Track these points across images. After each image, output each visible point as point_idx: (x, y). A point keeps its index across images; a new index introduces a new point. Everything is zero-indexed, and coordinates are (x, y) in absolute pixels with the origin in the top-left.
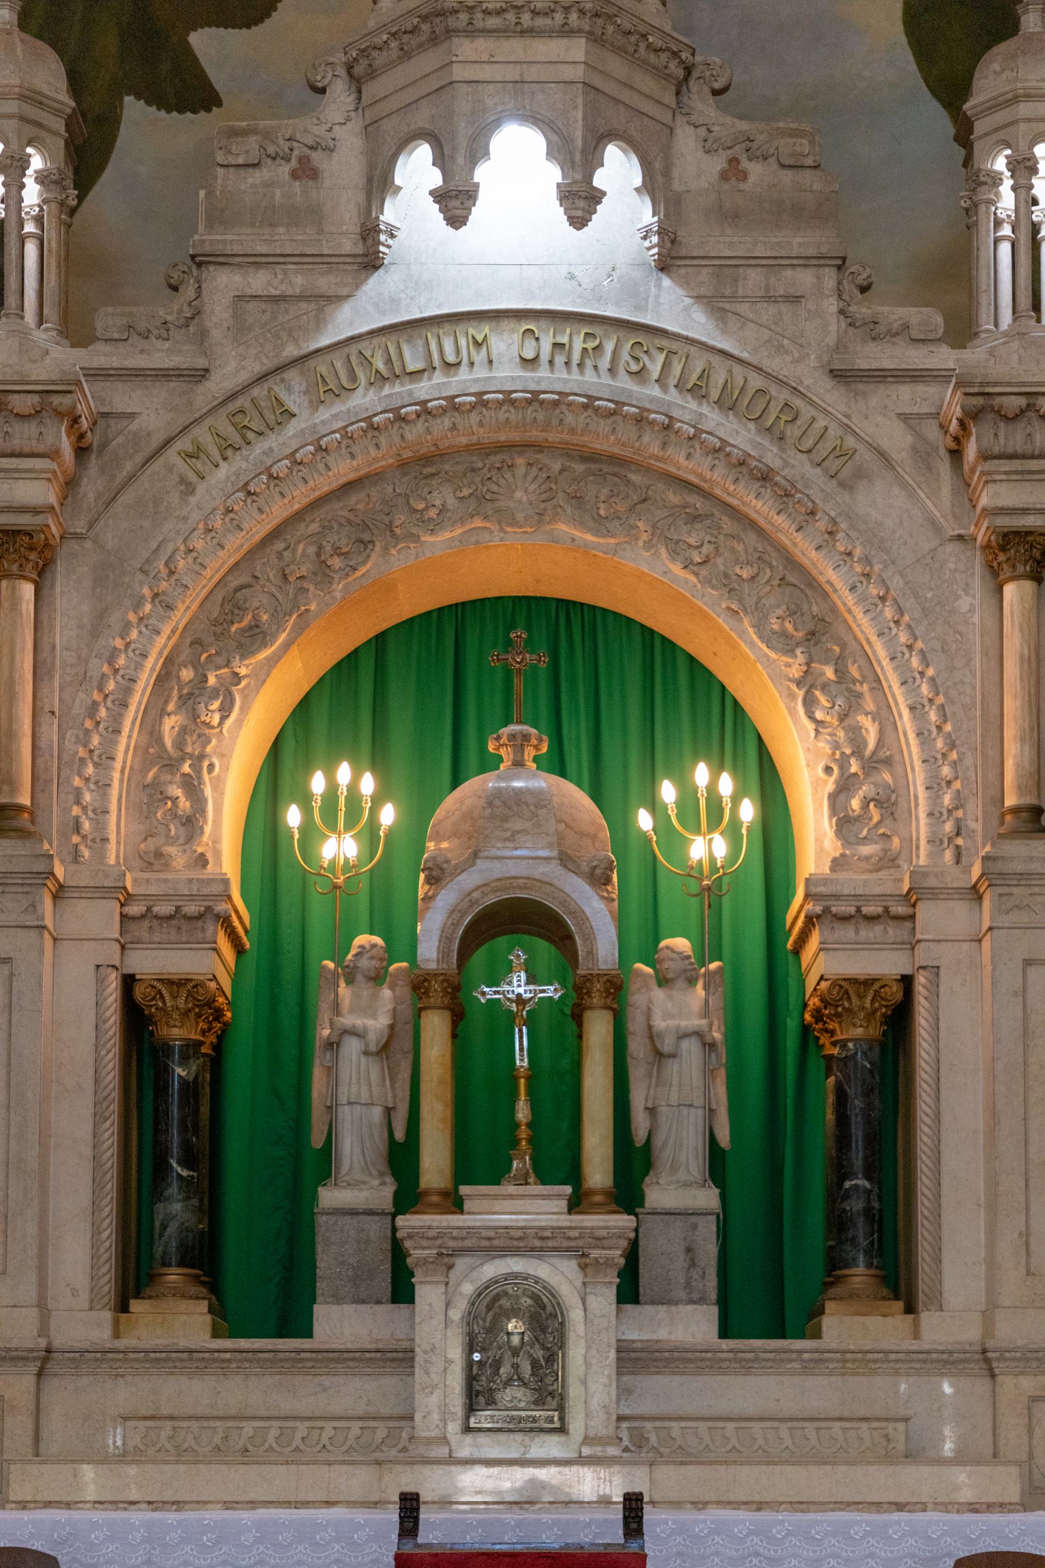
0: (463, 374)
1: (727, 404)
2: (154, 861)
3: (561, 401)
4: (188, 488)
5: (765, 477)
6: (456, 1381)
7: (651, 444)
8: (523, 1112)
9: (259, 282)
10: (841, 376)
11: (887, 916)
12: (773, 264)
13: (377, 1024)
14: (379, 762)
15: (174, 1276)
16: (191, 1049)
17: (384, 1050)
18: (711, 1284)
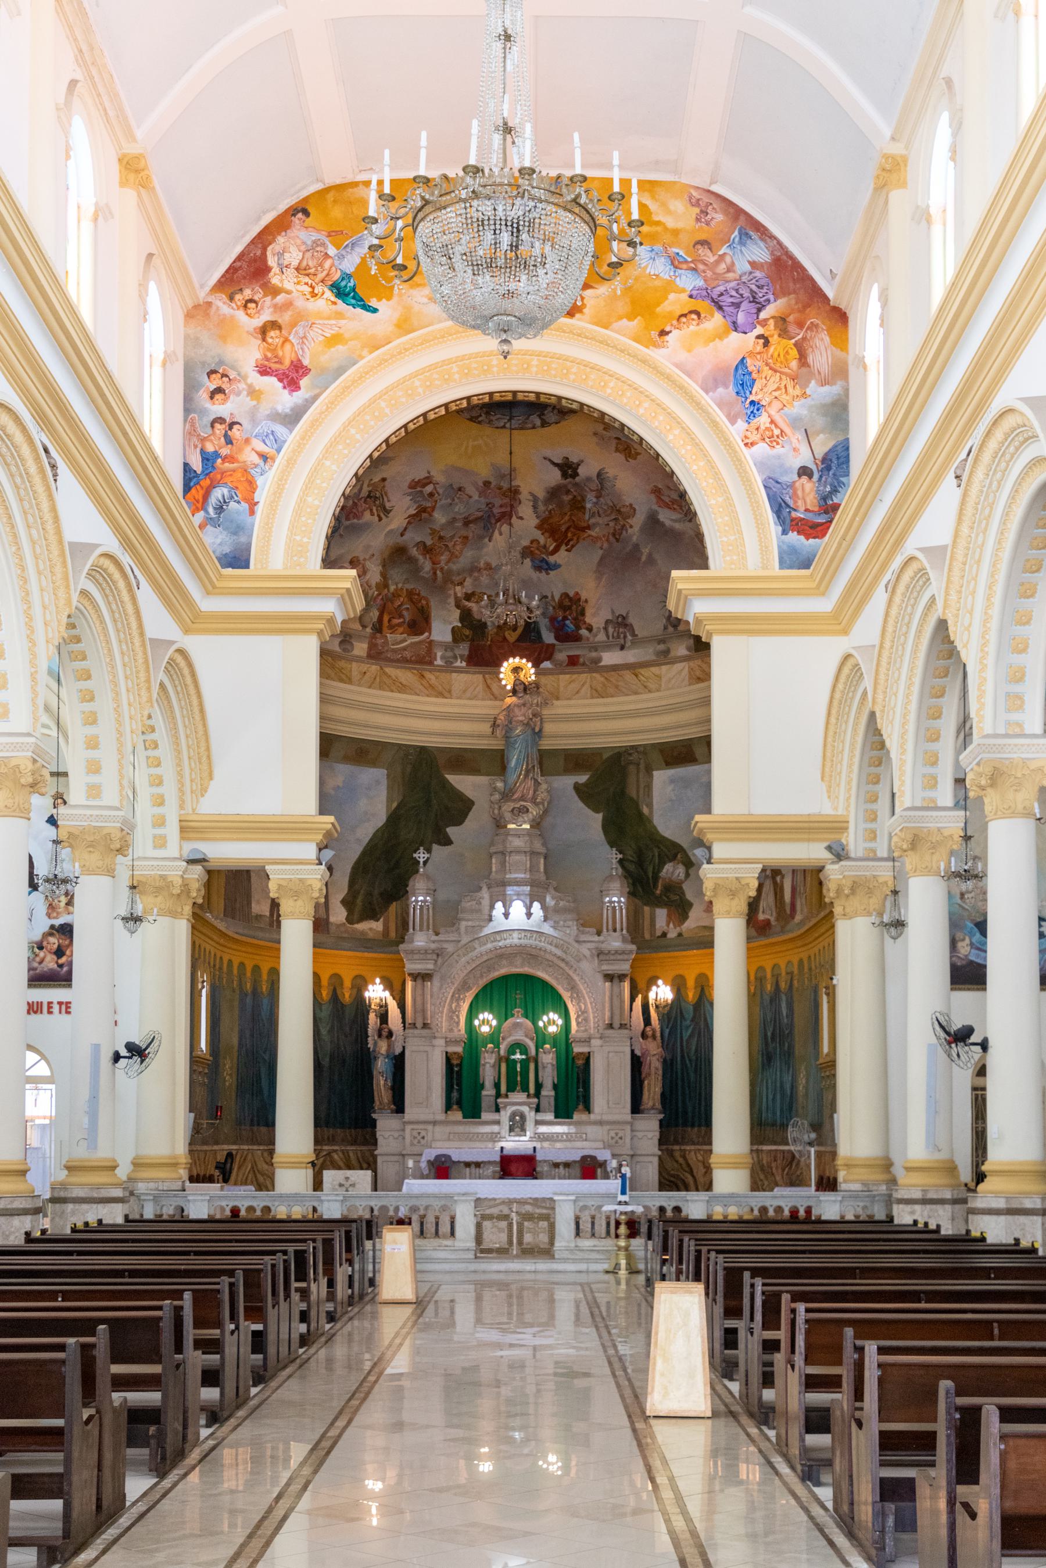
0: (508, 941)
1: (556, 946)
2: (451, 1030)
3: (526, 946)
4: (457, 962)
5: (563, 960)
6: (507, 1128)
7: (542, 953)
8: (519, 1079)
9: (470, 923)
10: (577, 941)
11: (585, 1041)
12: (565, 921)
13: (492, 1061)
14: (491, 1012)
15: (455, 1107)
16: (457, 1065)
17: (494, 1066)
18: (553, 1109)
